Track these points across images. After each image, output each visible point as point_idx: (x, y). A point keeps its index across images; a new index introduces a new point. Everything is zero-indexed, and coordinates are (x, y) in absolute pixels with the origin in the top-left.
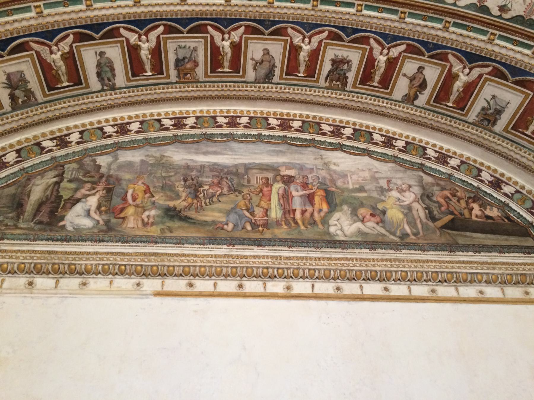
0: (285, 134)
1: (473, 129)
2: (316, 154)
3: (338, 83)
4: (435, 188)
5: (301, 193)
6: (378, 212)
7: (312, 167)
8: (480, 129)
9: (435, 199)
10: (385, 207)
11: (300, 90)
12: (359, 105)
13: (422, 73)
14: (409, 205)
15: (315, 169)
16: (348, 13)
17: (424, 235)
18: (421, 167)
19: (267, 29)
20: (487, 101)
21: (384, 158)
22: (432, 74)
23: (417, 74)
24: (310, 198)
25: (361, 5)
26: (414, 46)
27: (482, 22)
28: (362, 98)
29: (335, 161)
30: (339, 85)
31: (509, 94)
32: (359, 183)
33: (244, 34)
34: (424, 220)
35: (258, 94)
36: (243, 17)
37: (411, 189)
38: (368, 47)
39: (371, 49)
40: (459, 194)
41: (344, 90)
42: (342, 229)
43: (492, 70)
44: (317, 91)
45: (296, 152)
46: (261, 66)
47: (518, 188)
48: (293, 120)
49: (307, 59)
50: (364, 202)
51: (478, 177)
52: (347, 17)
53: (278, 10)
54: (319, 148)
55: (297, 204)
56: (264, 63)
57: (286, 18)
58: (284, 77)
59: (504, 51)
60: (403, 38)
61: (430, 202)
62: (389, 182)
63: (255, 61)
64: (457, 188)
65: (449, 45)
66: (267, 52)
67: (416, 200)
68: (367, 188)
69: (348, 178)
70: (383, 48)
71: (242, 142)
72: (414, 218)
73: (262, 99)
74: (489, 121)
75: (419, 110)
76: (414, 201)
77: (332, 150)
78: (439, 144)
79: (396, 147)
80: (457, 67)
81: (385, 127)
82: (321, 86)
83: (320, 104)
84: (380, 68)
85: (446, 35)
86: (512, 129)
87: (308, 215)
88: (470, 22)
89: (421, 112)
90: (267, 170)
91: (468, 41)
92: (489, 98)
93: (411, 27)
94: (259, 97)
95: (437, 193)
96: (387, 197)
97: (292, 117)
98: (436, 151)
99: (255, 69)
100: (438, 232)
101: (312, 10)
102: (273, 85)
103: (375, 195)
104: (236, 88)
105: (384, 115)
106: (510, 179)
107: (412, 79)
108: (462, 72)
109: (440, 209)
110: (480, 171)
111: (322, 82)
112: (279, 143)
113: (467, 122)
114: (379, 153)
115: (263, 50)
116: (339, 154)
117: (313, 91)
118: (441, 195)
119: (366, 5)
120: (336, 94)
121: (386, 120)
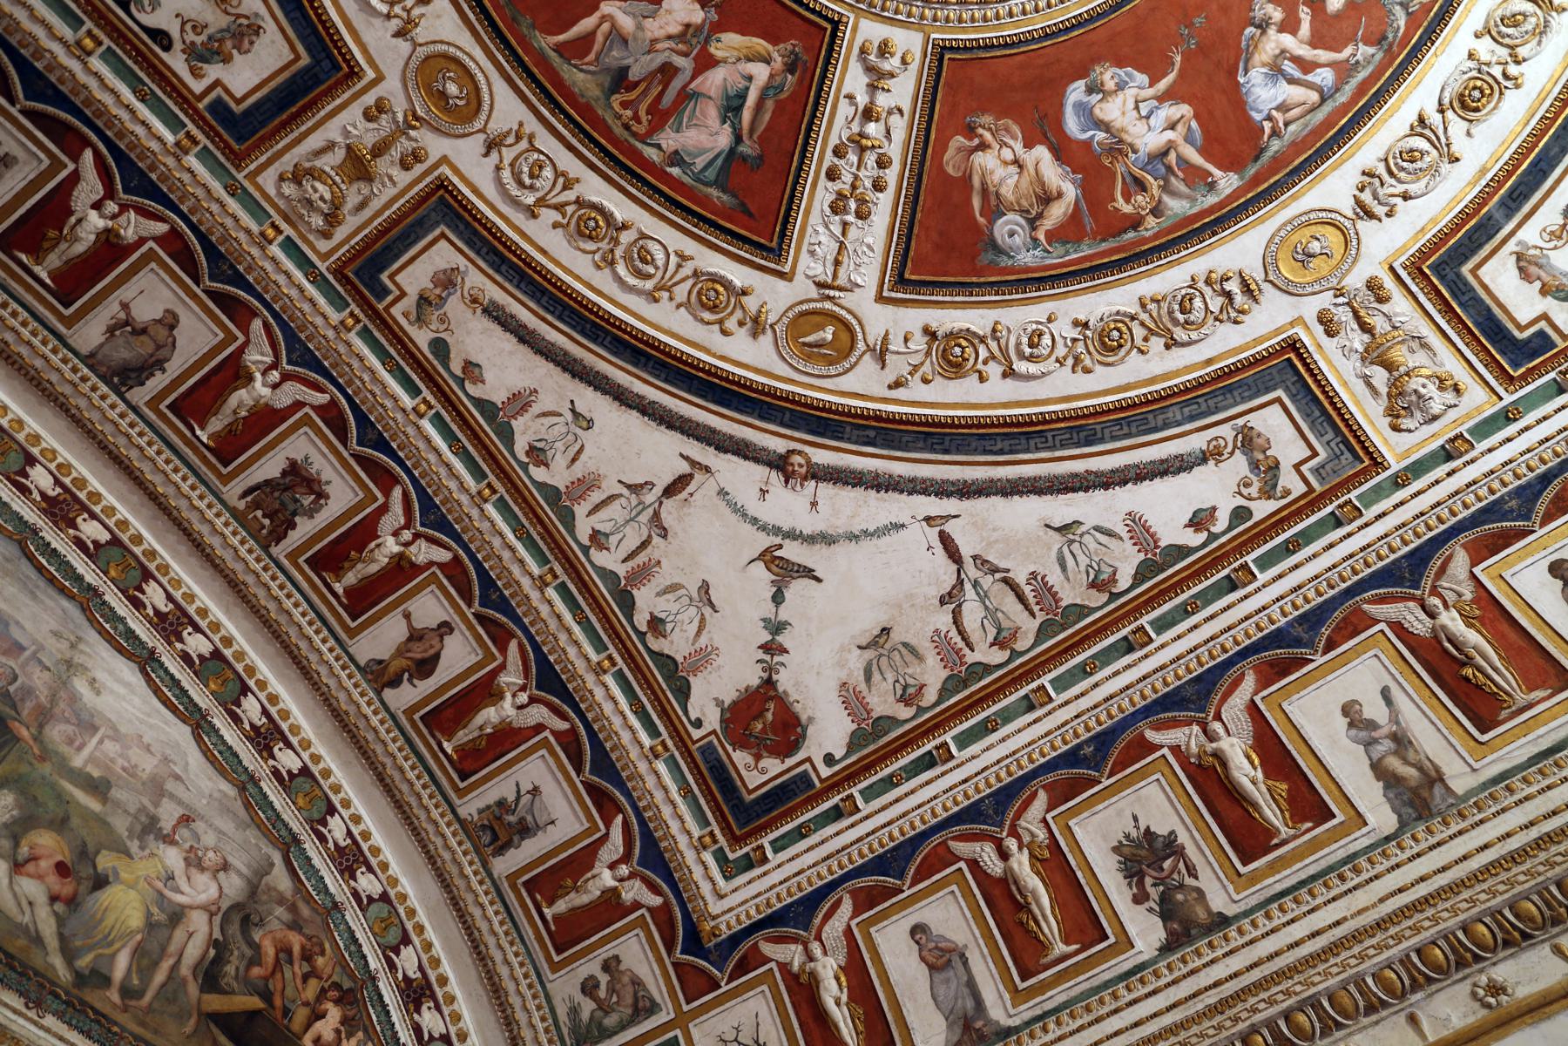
0: (40, 523)
1: (454, 834)
2: (71, 626)
3: (267, 522)
4: (280, 911)
6: (86, 871)
7: (24, 641)
8: (468, 845)
9: (257, 936)
10: (116, 874)
11: (171, 466)
12: (272, 606)
13: (441, 637)
14: (183, 907)
15: (27, 653)
16: (395, 400)
17: (149, 1009)
18: (289, 845)
19: (212, 278)
20: (518, 792)
21: (223, 761)
22: (459, 655)
23: (432, 634)
25: (430, 407)
26: (465, 571)
27: (608, 621)
28: (289, 596)
29: (100, 675)
30: (263, 527)
31: (564, 803)
32: (108, 768)
33: (155, 239)
34: (185, 970)
35: (67, 390)
36: (184, 208)
37: (221, 875)
38: (381, 500)
39: (384, 509)
40: (320, 961)
41: (266, 548)
43: (567, 731)
44: (206, 501)
45: (23, 584)
46: (132, 339)
47: (453, 1030)
48: (93, 516)
49: (244, 414)
50: (75, 822)
51: (390, 951)
52: (389, 403)
53: (268, 266)
54: (92, 621)
56: (143, 338)
57: (272, 293)
58: (162, 407)
59: (608, 708)
60: (457, 538)
61: (239, 937)
62: (186, 820)
63: (128, 314)
64: (327, 946)
65: (526, 620)
66: (170, 322)
67: (210, 910)
68: (116, 793)
69: (93, 735)
70: (407, 526)
72: (163, 949)
73: (67, 411)
74: (495, 838)
75: (383, 714)
76: (203, 908)
77: (120, 650)
78: (369, 822)
79: (274, 758)
80: (511, 678)
81: (288, 701)
82: (224, 497)
83: (189, 535)
84: (373, 561)
85: (535, 596)
86: (525, 884)
88: (589, 605)
89: (382, 722)
91: (563, 637)
92: (526, 786)
93: (485, 526)
94: (62, 399)
95: (275, 925)
96: (147, 852)
97: (97, 509)
98: (349, 833)
99: (111, 330)
100: (193, 1021)
101: (335, 328)
102: (119, 401)
103: (120, 824)
104: (25, 333)
105: (306, 672)
106: (451, 999)
107: (416, 636)
108: (514, 696)
109: (248, 968)
110: (406, 940)
111: (233, 491)
113: (454, 811)
114: (224, 743)
115: (167, 311)
116: (128, 672)
117: (198, 492)
118: (279, 935)
119: (437, 414)
120: (242, 542)
121: (303, 687)
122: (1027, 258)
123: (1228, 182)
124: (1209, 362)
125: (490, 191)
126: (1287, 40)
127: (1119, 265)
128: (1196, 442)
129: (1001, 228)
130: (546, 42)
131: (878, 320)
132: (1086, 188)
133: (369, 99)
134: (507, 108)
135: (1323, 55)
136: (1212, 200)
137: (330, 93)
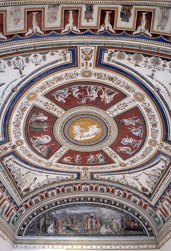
5: (95, 221)
24: (97, 222)
29: (103, 211)
42: (103, 231)
55: (94, 225)
71: (82, 206)
77: (102, 207)
87: (96, 227)
90: (87, 214)
112: (90, 206)
116: (104, 208)
122: (131, 153)
123: (141, 141)
124: (153, 154)
125: (94, 171)
126: (133, 129)
127: (138, 151)
128: (157, 161)
129: (127, 152)
130: (87, 163)
131: (126, 162)
132: (130, 147)
133: (82, 172)
134: (90, 167)
135: (138, 129)
136: (141, 143)
137: (80, 174)
